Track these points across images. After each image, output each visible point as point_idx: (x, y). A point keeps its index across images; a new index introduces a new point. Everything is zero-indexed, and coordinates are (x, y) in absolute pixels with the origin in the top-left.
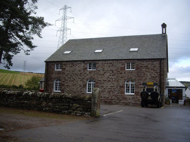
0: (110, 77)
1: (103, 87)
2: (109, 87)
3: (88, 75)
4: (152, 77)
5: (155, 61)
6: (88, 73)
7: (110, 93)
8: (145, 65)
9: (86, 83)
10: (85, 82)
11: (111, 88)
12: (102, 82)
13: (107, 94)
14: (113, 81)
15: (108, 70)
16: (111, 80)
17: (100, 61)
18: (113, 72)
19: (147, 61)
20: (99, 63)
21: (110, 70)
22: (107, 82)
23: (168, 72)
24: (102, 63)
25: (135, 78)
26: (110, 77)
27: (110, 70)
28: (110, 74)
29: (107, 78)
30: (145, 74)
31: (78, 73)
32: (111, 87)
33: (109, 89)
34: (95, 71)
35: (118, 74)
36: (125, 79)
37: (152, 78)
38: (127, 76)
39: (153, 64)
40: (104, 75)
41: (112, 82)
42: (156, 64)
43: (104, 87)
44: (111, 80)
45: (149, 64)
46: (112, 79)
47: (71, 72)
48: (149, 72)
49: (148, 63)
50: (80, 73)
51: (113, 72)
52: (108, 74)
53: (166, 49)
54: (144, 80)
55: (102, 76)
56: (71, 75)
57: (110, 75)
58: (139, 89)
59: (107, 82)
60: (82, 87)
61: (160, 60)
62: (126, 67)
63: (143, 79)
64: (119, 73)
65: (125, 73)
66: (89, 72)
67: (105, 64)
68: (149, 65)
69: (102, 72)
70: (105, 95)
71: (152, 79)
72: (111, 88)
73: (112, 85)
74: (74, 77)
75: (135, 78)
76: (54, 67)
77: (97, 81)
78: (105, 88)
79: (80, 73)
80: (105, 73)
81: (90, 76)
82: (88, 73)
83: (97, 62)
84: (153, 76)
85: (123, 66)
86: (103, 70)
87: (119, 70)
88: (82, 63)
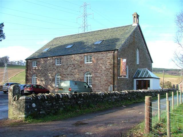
0: (73, 71)
3: (56, 70)
4: (107, 69)
5: (109, 53)
6: (55, 67)
8: (100, 58)
9: (54, 77)
12: (67, 75)
14: (74, 74)
15: (70, 65)
16: (73, 73)
17: (64, 56)
18: (74, 66)
19: (102, 54)
20: (64, 58)
21: (72, 64)
22: (69, 75)
24: (66, 58)
25: (92, 70)
26: (73, 71)
27: (72, 64)
28: (72, 68)
30: (100, 66)
31: (48, 68)
34: (61, 66)
35: (78, 67)
36: (84, 72)
37: (106, 70)
38: (86, 69)
39: (107, 56)
40: (67, 69)
41: (74, 76)
42: (110, 55)
44: (73, 73)
45: (104, 56)
46: (74, 72)
47: (43, 68)
48: (103, 64)
49: (103, 55)
50: (50, 69)
51: (74, 66)
52: (71, 68)
53: (140, 34)
54: (100, 72)
55: (66, 70)
56: (44, 71)
57: (72, 69)
58: (96, 81)
60: (52, 81)
61: (113, 52)
62: (85, 60)
63: (99, 71)
64: (79, 66)
65: (84, 66)
66: (56, 67)
67: (68, 58)
68: (104, 58)
69: (66, 67)
71: (107, 71)
74: (46, 72)
75: (92, 70)
76: (32, 64)
77: (62, 75)
80: (68, 67)
81: (57, 71)
82: (55, 67)
83: (62, 57)
84: (107, 68)
85: (82, 60)
86: (67, 65)
87: (79, 64)
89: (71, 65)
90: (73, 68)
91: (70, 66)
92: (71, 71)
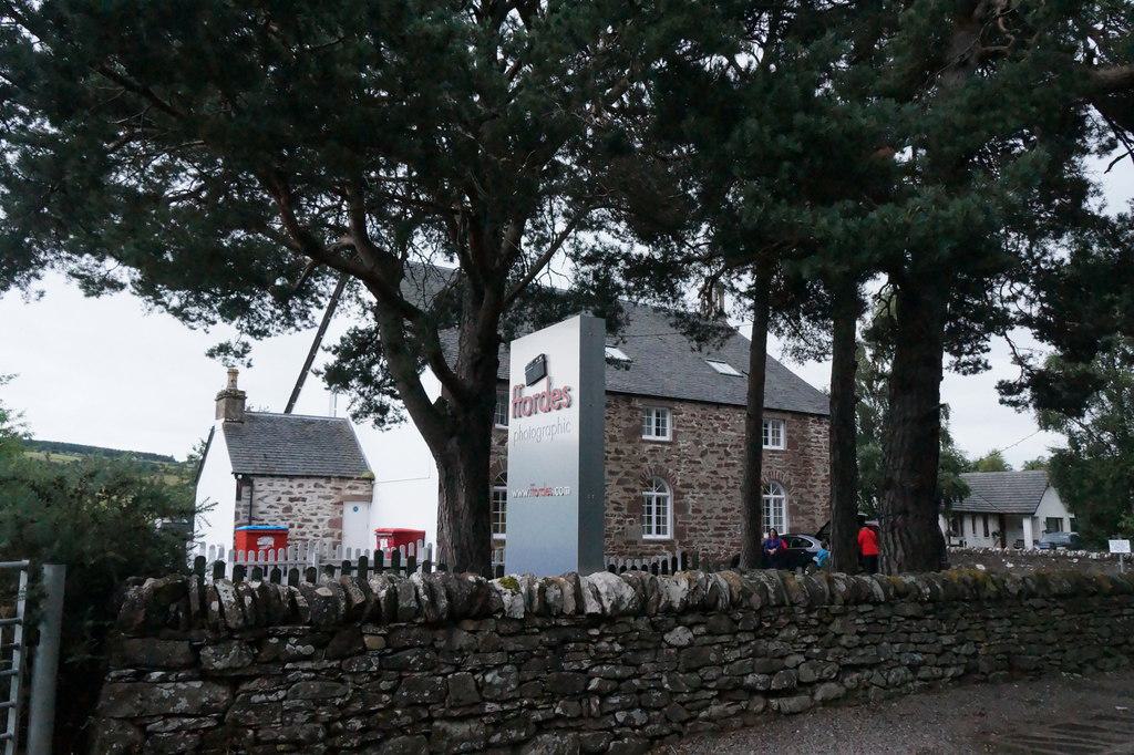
1: (700, 511)
2: (719, 512)
7: (720, 535)
11: (724, 514)
13: (714, 539)
14: (728, 487)
16: (723, 483)
22: (710, 490)
29: (712, 475)
32: (725, 510)
33: (718, 518)
41: (726, 493)
43: (704, 513)
50: (617, 451)
57: (719, 466)
59: (710, 490)
70: (706, 546)
72: (724, 514)
73: (725, 504)
78: (704, 518)
79: (617, 451)
89: (715, 449)
90: (723, 462)
91: (712, 452)
92: (715, 472)
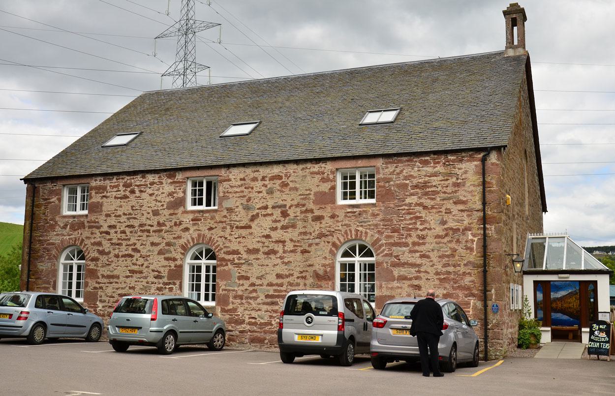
1: (247, 278)
2: (272, 278)
3: (187, 229)
5: (461, 161)
6: (187, 219)
7: (273, 303)
8: (415, 181)
9: (178, 263)
10: (175, 260)
11: (279, 281)
12: (245, 256)
13: (265, 307)
14: (284, 252)
15: (266, 208)
16: (279, 248)
17: (235, 171)
18: (285, 214)
19: (426, 163)
20: (231, 177)
21: (273, 207)
22: (260, 255)
23: (545, 210)
24: (244, 179)
25: (377, 236)
26: (275, 235)
27: (273, 207)
28: (275, 221)
29: (264, 240)
30: (417, 218)
31: (149, 222)
32: (279, 276)
33: (270, 285)
36: (334, 245)
37: (446, 235)
38: (343, 229)
39: (450, 175)
40: (250, 227)
41: (281, 258)
42: (466, 172)
43: (253, 280)
44: (279, 248)
45: (435, 175)
46: (284, 242)
47: (123, 219)
48: (433, 207)
50: (159, 224)
51: (285, 214)
52: (267, 223)
54: (414, 244)
55: (244, 232)
56: (124, 232)
57: (274, 229)
58: (395, 284)
59: (260, 255)
60: (165, 280)
61: (481, 156)
63: (410, 241)
64: (310, 215)
65: (333, 217)
66: (191, 216)
67: (255, 179)
68: (435, 181)
70: (254, 314)
72: (279, 281)
73: (282, 269)
74: (133, 241)
75: (377, 236)
76: (60, 200)
78: (253, 285)
79: (159, 224)
80: (253, 218)
81: (195, 235)
82: (187, 219)
83: (223, 172)
84: (451, 224)
85: (325, 187)
86: (247, 208)
87: (311, 206)
88: (166, 181)
89: (269, 211)
90: (279, 225)
91: (265, 216)
92: (268, 237)
